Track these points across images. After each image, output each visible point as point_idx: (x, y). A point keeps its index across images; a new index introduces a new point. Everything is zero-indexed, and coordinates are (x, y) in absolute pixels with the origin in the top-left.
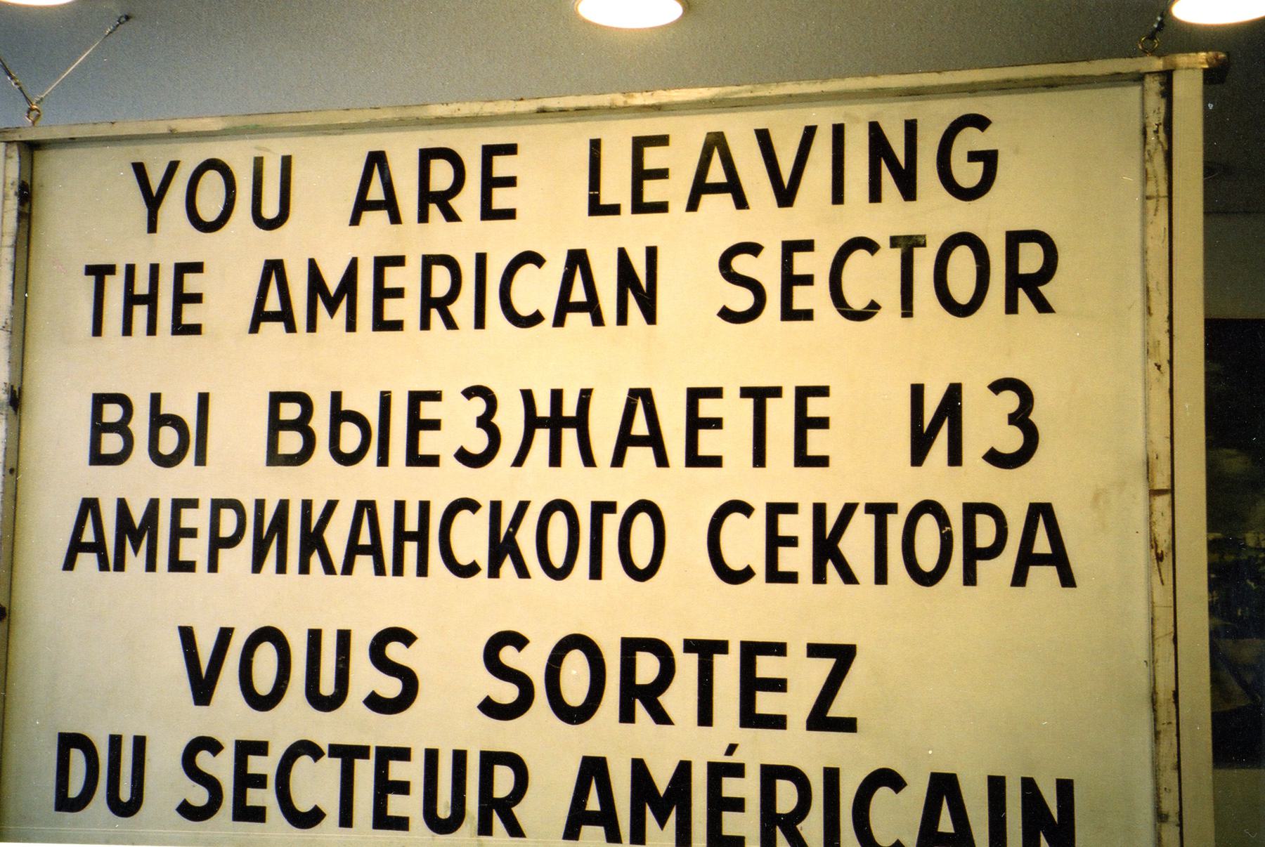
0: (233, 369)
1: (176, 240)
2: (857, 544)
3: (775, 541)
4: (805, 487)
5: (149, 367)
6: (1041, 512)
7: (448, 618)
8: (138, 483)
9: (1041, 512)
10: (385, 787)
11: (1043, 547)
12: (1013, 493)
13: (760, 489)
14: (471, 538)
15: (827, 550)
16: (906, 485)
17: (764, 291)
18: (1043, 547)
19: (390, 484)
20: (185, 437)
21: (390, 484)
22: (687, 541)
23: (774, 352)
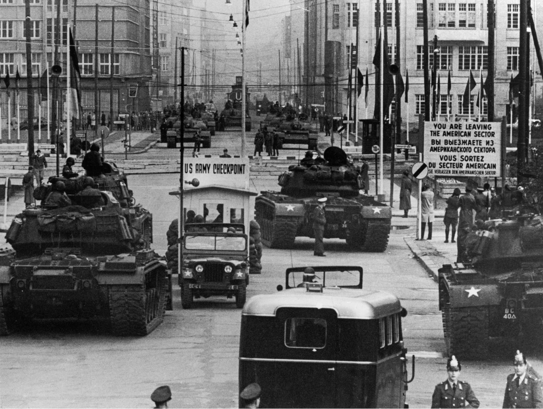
0: (442, 138)
1: (437, 129)
2: (483, 150)
3: (478, 150)
4: (480, 146)
5: (436, 138)
6: (494, 148)
7: (458, 155)
8: (435, 146)
9: (494, 148)
10: (453, 165)
11: (494, 150)
12: (492, 147)
13: (477, 146)
14: (459, 150)
15: (481, 151)
16: (486, 146)
17: (477, 135)
18: (494, 150)
19: (453, 146)
20: (439, 142)
21: (453, 146)
22: (473, 149)
23: (478, 138)
